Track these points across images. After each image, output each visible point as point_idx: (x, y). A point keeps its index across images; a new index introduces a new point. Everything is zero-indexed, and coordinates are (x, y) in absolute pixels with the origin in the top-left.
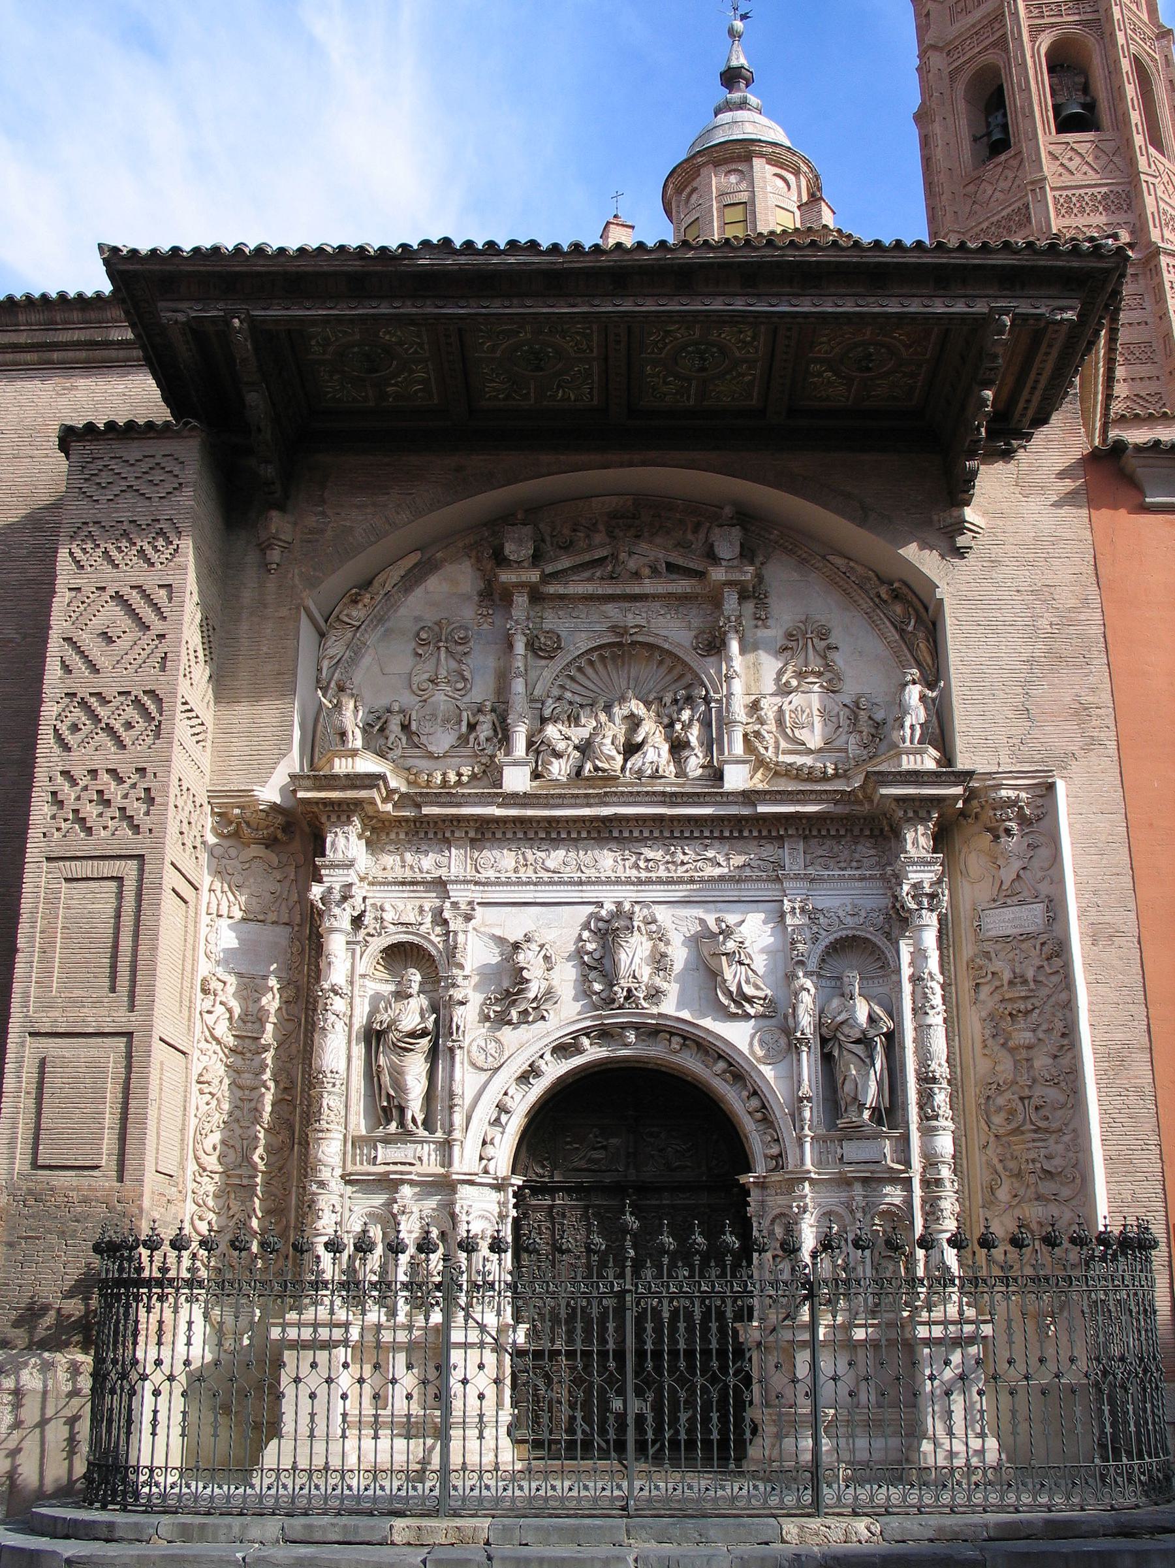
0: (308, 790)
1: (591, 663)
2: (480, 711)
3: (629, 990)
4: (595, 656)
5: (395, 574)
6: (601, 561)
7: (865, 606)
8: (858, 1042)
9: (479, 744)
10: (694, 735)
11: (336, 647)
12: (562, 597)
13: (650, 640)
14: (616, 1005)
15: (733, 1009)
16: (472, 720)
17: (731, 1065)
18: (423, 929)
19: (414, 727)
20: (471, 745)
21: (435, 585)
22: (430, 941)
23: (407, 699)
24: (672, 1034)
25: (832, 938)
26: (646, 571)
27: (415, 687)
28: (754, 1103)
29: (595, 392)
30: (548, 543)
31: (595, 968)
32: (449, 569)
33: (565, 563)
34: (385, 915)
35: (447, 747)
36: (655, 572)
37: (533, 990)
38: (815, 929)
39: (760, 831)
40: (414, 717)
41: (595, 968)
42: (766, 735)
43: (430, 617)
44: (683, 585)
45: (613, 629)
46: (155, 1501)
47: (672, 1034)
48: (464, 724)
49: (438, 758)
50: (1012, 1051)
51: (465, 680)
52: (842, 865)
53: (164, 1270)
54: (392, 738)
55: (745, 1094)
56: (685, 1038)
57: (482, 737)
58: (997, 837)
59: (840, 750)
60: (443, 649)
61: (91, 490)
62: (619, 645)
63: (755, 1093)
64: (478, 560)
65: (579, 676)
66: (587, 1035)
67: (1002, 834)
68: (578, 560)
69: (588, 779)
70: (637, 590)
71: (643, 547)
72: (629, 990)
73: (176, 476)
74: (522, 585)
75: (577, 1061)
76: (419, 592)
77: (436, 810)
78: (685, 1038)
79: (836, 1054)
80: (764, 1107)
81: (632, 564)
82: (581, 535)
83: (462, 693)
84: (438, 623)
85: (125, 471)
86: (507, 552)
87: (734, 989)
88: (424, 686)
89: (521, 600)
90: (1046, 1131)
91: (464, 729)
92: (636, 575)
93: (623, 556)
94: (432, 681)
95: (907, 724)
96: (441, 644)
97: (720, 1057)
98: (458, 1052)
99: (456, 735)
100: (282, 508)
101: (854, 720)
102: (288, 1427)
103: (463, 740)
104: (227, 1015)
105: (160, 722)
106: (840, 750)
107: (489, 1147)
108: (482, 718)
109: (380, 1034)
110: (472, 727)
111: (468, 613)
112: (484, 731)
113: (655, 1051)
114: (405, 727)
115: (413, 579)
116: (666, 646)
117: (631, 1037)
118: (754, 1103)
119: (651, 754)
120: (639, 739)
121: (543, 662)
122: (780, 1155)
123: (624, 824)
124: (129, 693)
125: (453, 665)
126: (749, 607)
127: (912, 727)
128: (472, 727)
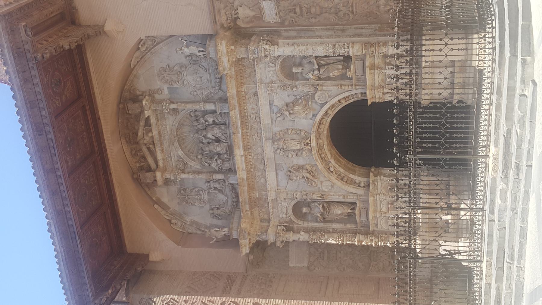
1: (186, 147)
4: (183, 146)
5: (163, 213)
6: (149, 149)
11: (192, 230)
12: (164, 160)
14: (310, 148)
16: (213, 189)
17: (329, 108)
18: (287, 206)
20: (222, 188)
23: (207, 207)
24: (319, 127)
26: (150, 135)
27: (203, 205)
30: (144, 164)
31: (297, 153)
33: (150, 160)
35: (224, 196)
36: (151, 131)
39: (243, 100)
40: (214, 206)
41: (297, 153)
42: (206, 93)
44: (153, 120)
48: (214, 192)
49: (227, 198)
50: (322, 13)
51: (199, 191)
52: (253, 71)
54: (223, 213)
55: (339, 104)
59: (208, 66)
60: (189, 197)
65: (191, 151)
69: (230, 156)
71: (140, 134)
74: (162, 176)
76: (169, 204)
77: (248, 206)
78: (320, 123)
82: (139, 154)
83: (203, 190)
84: (179, 198)
88: (202, 203)
92: (152, 137)
93: (145, 142)
94: (200, 200)
95: (198, 54)
96: (187, 198)
100: (148, 256)
103: (220, 191)
106: (208, 66)
108: (212, 186)
109: (324, 218)
114: (218, 209)
115: (165, 207)
116: (177, 125)
117: (320, 141)
118: (342, 101)
119: (219, 135)
121: (189, 166)
123: (245, 145)
126: (157, 96)
127: (199, 51)
128: (215, 189)
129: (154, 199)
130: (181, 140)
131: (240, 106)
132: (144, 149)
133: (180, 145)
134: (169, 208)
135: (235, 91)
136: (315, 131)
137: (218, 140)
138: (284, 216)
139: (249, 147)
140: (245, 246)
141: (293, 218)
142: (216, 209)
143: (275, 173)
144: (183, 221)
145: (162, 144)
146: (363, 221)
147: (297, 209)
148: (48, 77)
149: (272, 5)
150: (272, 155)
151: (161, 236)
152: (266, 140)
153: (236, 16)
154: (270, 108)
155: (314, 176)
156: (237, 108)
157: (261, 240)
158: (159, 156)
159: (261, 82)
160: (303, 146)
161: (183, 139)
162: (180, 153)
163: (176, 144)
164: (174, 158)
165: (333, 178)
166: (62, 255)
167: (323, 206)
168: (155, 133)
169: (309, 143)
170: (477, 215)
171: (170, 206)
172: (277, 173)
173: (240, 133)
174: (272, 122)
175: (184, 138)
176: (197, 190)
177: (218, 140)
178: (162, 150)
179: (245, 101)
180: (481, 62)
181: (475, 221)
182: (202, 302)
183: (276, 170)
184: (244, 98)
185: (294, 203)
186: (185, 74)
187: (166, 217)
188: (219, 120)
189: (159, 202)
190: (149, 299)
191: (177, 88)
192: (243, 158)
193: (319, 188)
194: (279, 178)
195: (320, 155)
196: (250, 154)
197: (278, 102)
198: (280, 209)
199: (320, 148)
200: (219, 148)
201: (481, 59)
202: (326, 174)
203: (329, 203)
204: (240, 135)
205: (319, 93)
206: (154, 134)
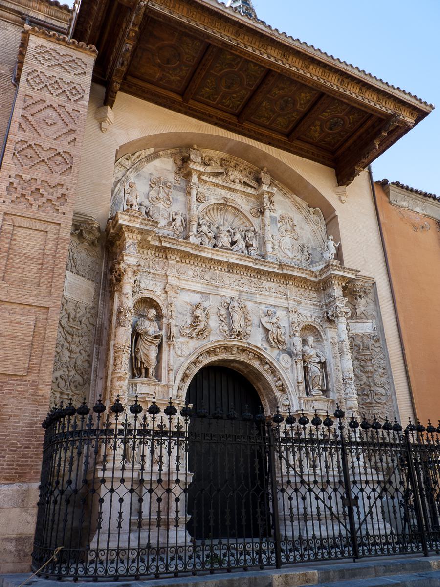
0: (124, 220)
2: (176, 214)
3: (239, 332)
6: (221, 173)
7: (304, 214)
8: (319, 363)
9: (176, 227)
10: (254, 243)
12: (206, 182)
13: (236, 206)
14: (233, 337)
15: (273, 344)
16: (174, 218)
19: (151, 213)
21: (157, 163)
22: (160, 299)
24: (250, 352)
25: (304, 324)
26: (237, 181)
27: (150, 199)
28: (280, 383)
29: (240, 106)
32: (163, 159)
34: (141, 285)
37: (202, 326)
38: (299, 320)
40: (151, 210)
43: (156, 175)
44: (249, 190)
45: (225, 199)
46: (100, 573)
47: (250, 352)
48: (171, 217)
51: (169, 200)
53: (145, 424)
56: (255, 354)
57: (178, 225)
58: (356, 299)
59: (299, 260)
61: (40, 58)
62: (225, 205)
63: (280, 379)
64: (175, 160)
66: (219, 348)
67: (358, 297)
68: (213, 170)
70: (233, 187)
72: (239, 332)
73: (83, 69)
75: (214, 358)
77: (168, 245)
78: (255, 354)
79: (309, 366)
80: (282, 385)
81: (232, 177)
84: (159, 178)
85: (57, 57)
86: (191, 158)
87: (275, 337)
89: (194, 179)
90: (380, 403)
91: (171, 219)
94: (157, 198)
97: (267, 363)
98: (172, 347)
99: (168, 221)
100: (111, 107)
101: (302, 250)
102: (104, 525)
103: (170, 224)
104: (67, 316)
105: (71, 167)
107: (180, 391)
110: (174, 220)
111: (171, 178)
112: (178, 222)
113: (242, 357)
116: (241, 210)
118: (280, 383)
120: (235, 240)
122: (289, 405)
124: (56, 150)
125: (165, 195)
128: (174, 220)
129: (161, 152)
130: (223, 207)
131: (277, 275)
132: (221, 170)
133: (218, 204)
134: (148, 162)
135: (296, 274)
136: (250, 347)
137: (233, 243)
138: (142, 285)
139: (231, 271)
140: (130, 221)
141: (140, 296)
142: (147, 211)
143: (199, 289)
144: (132, 168)
145: (223, 187)
146: (136, 386)
147: (150, 303)
148: (350, 120)
149: (369, 331)
150: (222, 293)
151: (135, 135)
152: (240, 291)
153: (358, 297)
154: (271, 305)
155: (198, 334)
156: (279, 271)
157: (127, 245)
158: (213, 179)
159: (299, 303)
160: (238, 329)
161: (220, 211)
162: (213, 202)
163: (222, 202)
164: (207, 194)
165: (192, 358)
166: (229, 14)
167: (156, 337)
168: (238, 187)
169: (239, 338)
170: (178, 561)
171: (149, 164)
172: (197, 292)
173: (254, 266)
174: (257, 303)
175: (222, 212)
176: (171, 200)
177: (233, 243)
178: (216, 185)
179: (278, 281)
180: (136, 554)
181: (146, 560)
182: (75, 131)
183: (202, 293)
184: (281, 282)
185: (160, 303)
186: (292, 237)
187: (137, 154)
188: (252, 252)
189: (155, 156)
190: (85, 73)
191: (277, 225)
192: (225, 260)
193: (179, 338)
194: (192, 294)
195: (219, 348)
196: (223, 270)
197: (281, 313)
198: (151, 283)
199: (226, 348)
200: (225, 240)
201: (100, 555)
202: (200, 351)
203: (160, 347)
204: (251, 265)
205: (290, 360)
206: (237, 185)
